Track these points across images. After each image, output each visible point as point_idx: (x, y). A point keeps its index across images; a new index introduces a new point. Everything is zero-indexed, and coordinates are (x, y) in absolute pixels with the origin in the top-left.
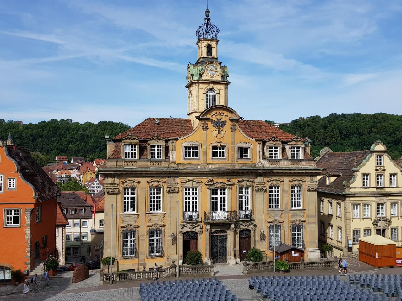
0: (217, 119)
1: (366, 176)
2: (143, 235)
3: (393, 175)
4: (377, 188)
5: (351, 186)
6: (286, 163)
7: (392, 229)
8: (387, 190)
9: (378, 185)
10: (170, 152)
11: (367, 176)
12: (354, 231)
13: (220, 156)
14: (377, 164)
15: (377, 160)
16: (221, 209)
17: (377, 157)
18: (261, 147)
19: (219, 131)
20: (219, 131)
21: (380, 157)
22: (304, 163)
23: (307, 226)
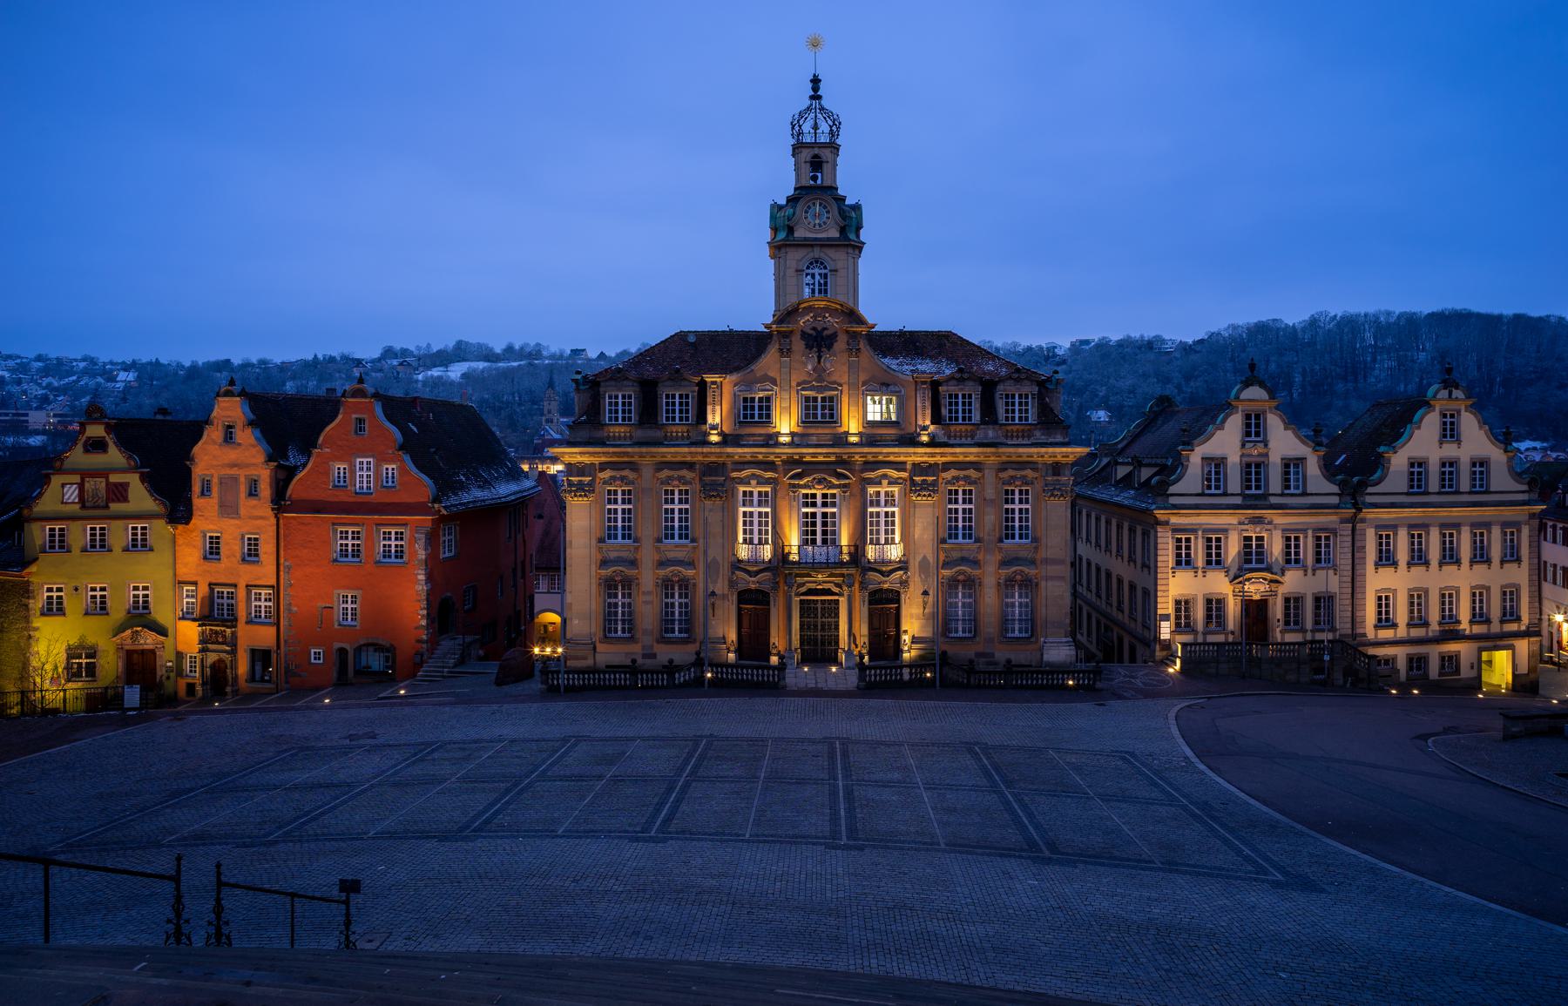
0: (814, 329)
1: (1216, 465)
2: (649, 593)
3: (1292, 465)
4: (1245, 497)
5: (1172, 490)
6: (991, 433)
7: (1287, 600)
8: (1273, 500)
9: (1249, 488)
10: (709, 408)
11: (1217, 466)
12: (1178, 602)
13: (823, 415)
14: (1248, 434)
15: (1248, 425)
16: (825, 541)
17: (1248, 417)
18: (929, 394)
19: (819, 358)
20: (819, 358)
21: (1258, 417)
22: (1038, 433)
23: (1043, 584)
